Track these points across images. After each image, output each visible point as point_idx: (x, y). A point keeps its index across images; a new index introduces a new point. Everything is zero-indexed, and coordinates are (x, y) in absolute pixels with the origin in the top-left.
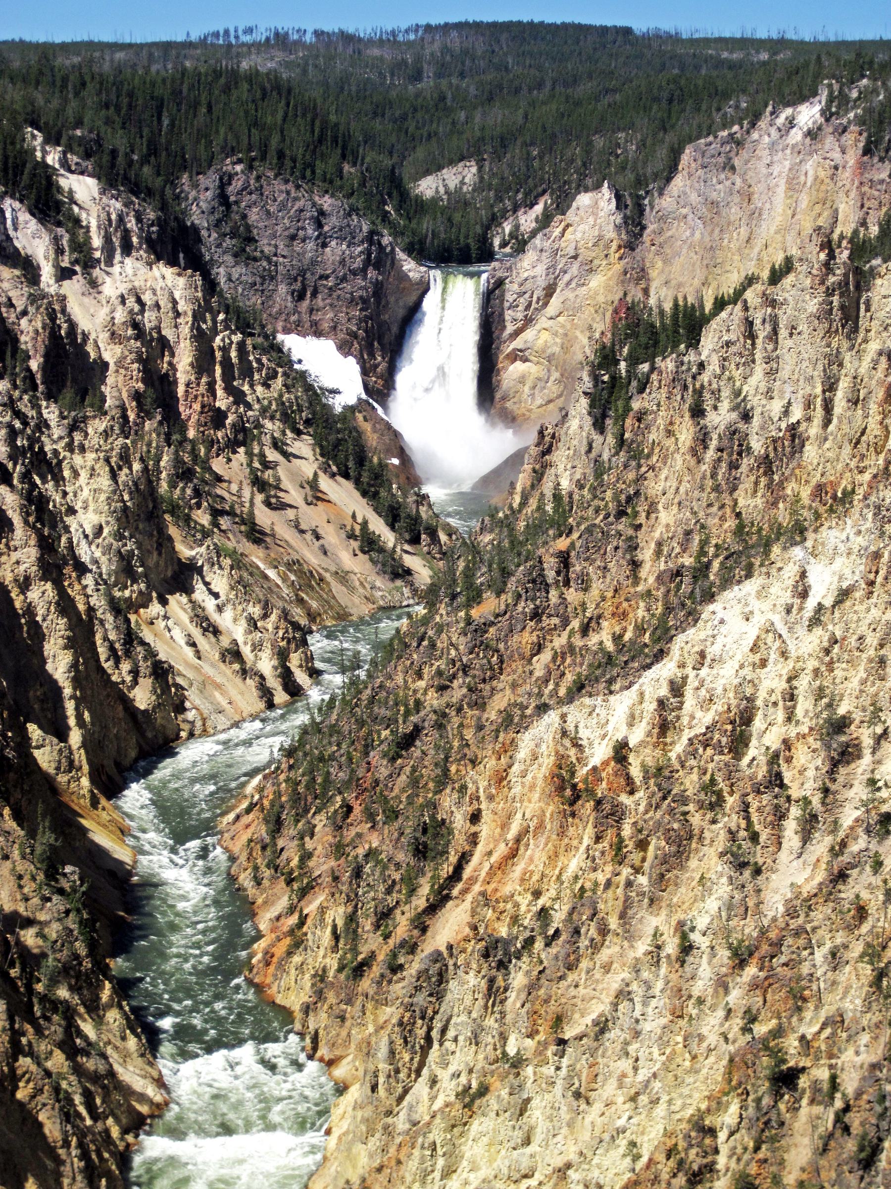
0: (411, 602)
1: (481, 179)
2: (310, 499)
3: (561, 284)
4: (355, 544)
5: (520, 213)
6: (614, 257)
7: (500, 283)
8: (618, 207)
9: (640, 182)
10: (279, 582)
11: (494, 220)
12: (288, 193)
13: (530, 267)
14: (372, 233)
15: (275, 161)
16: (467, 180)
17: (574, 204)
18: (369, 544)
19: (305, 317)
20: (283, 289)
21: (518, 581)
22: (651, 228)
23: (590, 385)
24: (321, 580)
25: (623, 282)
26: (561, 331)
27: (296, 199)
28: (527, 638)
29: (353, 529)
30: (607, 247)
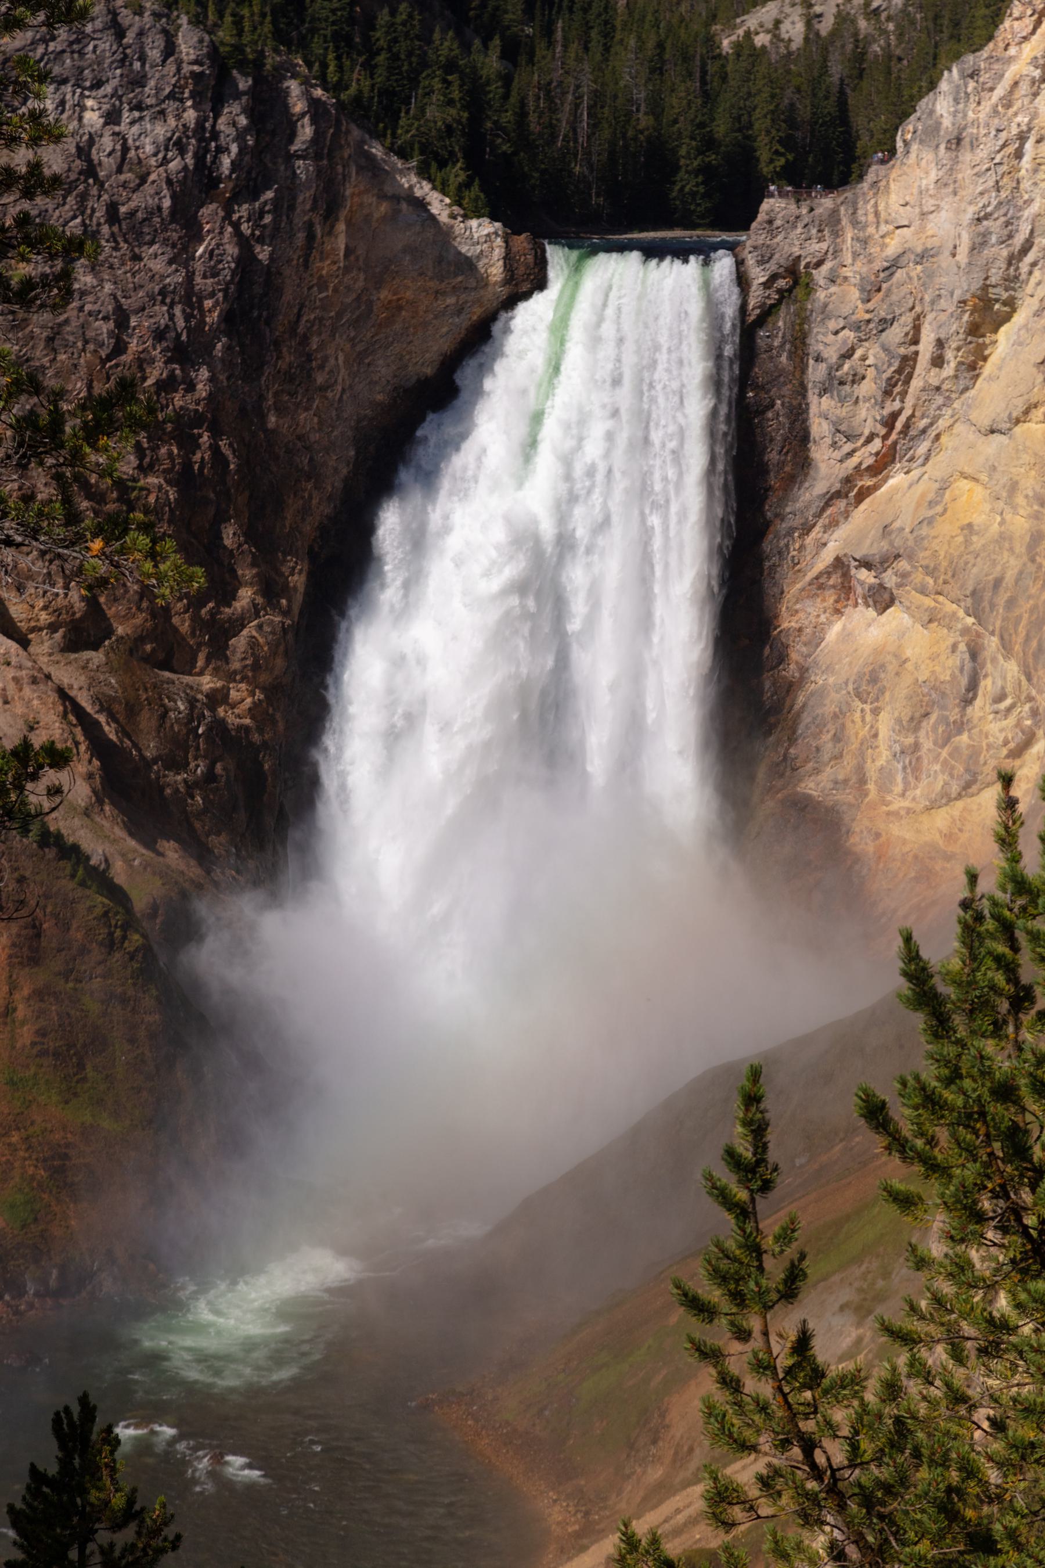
7: (794, 281)
26: (1029, 483)
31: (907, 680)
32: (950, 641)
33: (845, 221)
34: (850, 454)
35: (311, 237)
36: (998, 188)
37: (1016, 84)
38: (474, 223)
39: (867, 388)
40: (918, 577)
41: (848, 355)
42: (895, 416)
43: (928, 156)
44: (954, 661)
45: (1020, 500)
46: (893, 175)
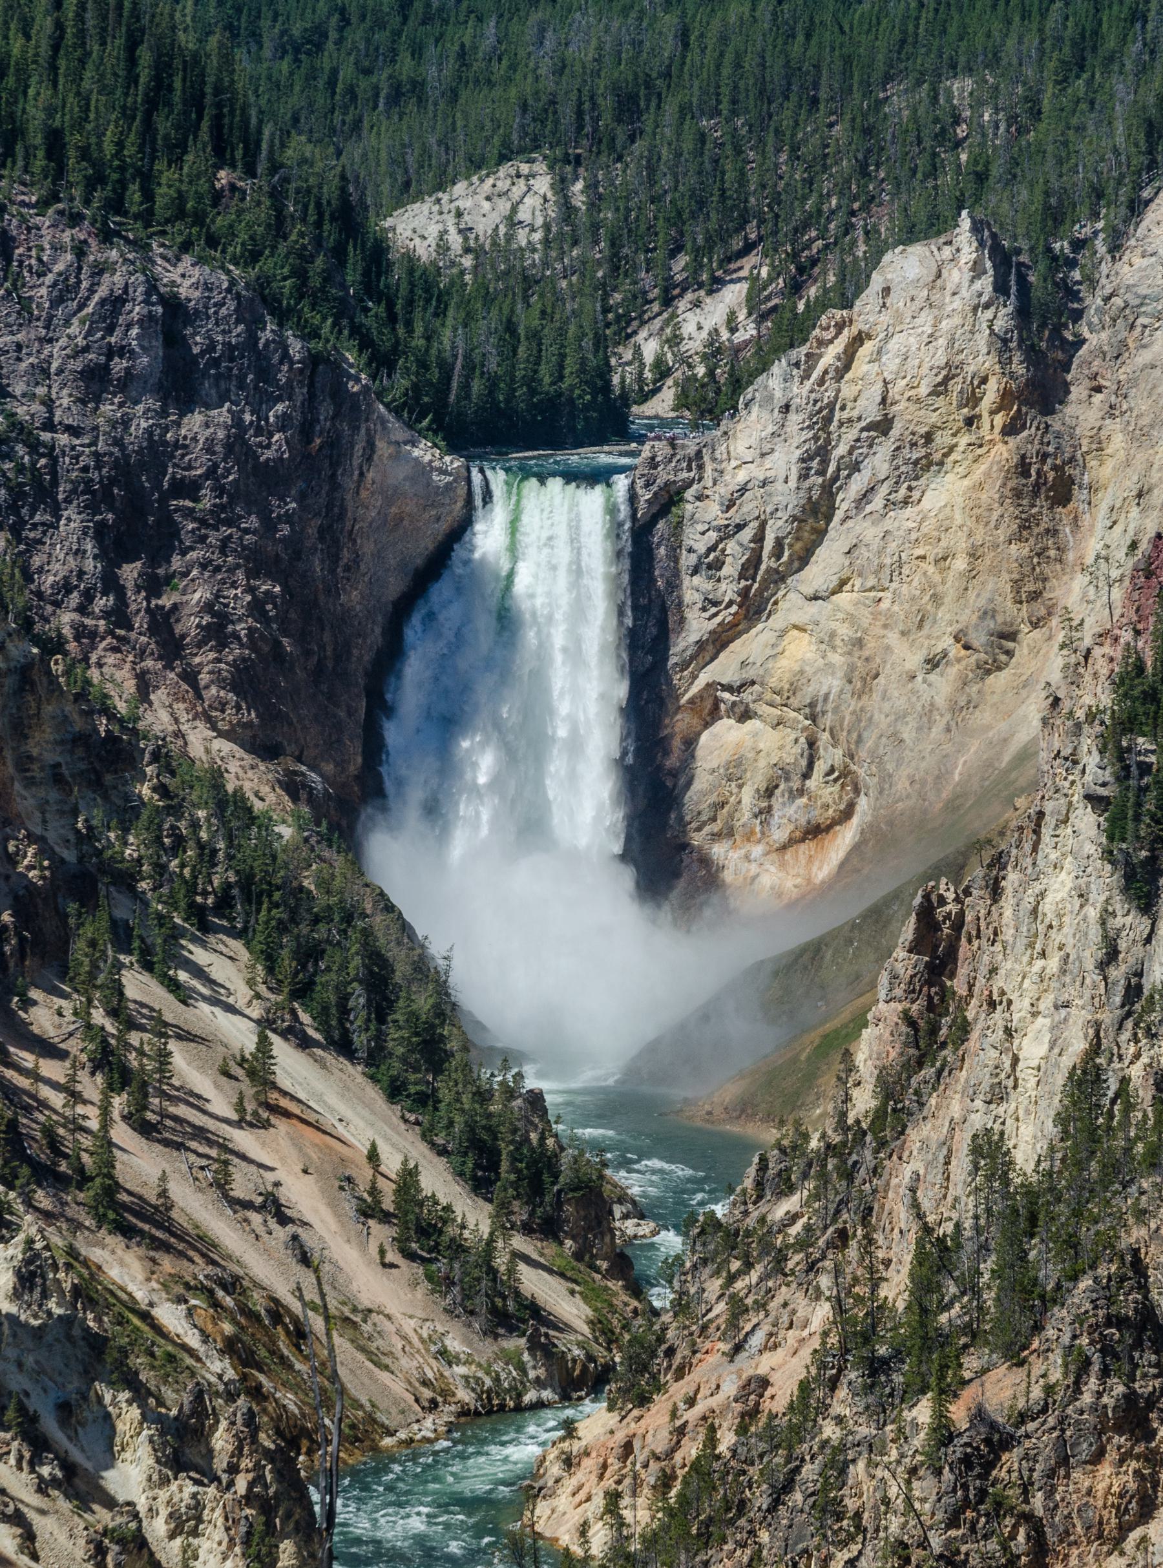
0: (547, 1394)
1: (567, 209)
2: (250, 1106)
3: (844, 502)
4: (381, 1233)
5: (682, 305)
6: (992, 424)
7: (669, 500)
8: (1001, 288)
9: (1055, 216)
10: (193, 1340)
11: (623, 328)
12: (80, 251)
13: (757, 454)
14: (314, 360)
15: (39, 163)
16: (523, 214)
17: (877, 280)
18: (420, 1234)
19: (137, 601)
20: (72, 521)
21: (1079, 1319)
22: (1095, 338)
23: (1107, 776)
24: (300, 1334)
25: (1018, 494)
26: (844, 631)
27: (99, 270)
28: (1109, 1479)
29: (374, 1191)
30: (972, 399)
31: (762, 763)
32: (793, 736)
33: (706, 458)
34: (715, 615)
35: (362, 474)
36: (816, 438)
37: (826, 372)
38: (448, 459)
39: (726, 570)
40: (768, 696)
41: (713, 548)
42: (748, 589)
43: (765, 415)
44: (797, 750)
45: (838, 642)
46: (740, 426)
